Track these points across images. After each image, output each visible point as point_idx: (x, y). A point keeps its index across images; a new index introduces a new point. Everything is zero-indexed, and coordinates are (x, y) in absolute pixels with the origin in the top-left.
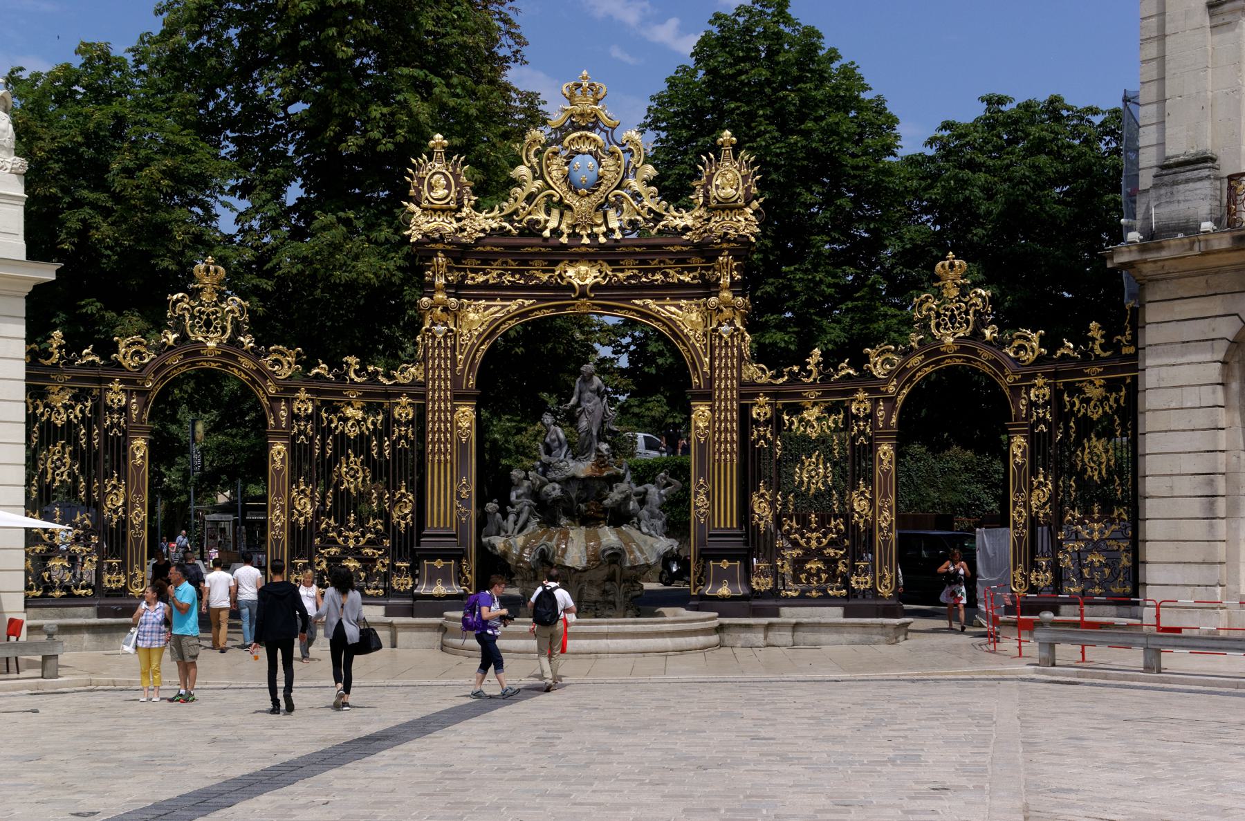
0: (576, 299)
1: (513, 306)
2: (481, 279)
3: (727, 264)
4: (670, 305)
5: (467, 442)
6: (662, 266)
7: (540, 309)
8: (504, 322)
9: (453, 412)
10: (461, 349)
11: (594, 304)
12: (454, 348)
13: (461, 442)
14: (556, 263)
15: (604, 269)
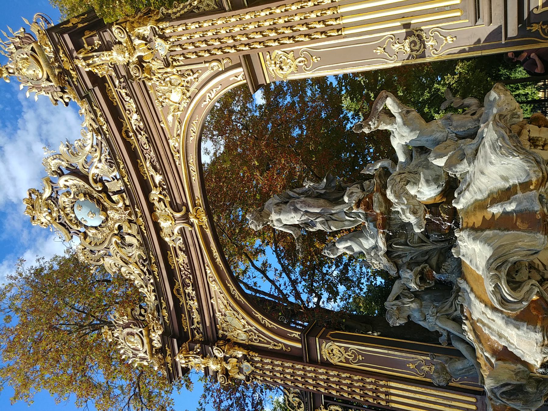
0: (192, 225)
1: (213, 286)
2: (196, 316)
3: (85, 59)
4: (167, 121)
5: (363, 355)
6: (131, 134)
7: (213, 259)
8: (233, 296)
9: (326, 364)
10: (263, 343)
11: (194, 205)
12: (263, 352)
13: (363, 361)
14: (164, 245)
15: (156, 198)
